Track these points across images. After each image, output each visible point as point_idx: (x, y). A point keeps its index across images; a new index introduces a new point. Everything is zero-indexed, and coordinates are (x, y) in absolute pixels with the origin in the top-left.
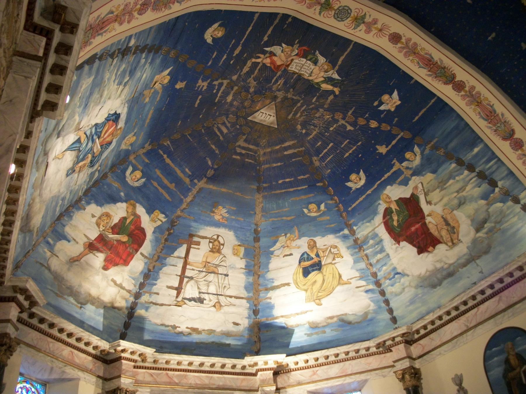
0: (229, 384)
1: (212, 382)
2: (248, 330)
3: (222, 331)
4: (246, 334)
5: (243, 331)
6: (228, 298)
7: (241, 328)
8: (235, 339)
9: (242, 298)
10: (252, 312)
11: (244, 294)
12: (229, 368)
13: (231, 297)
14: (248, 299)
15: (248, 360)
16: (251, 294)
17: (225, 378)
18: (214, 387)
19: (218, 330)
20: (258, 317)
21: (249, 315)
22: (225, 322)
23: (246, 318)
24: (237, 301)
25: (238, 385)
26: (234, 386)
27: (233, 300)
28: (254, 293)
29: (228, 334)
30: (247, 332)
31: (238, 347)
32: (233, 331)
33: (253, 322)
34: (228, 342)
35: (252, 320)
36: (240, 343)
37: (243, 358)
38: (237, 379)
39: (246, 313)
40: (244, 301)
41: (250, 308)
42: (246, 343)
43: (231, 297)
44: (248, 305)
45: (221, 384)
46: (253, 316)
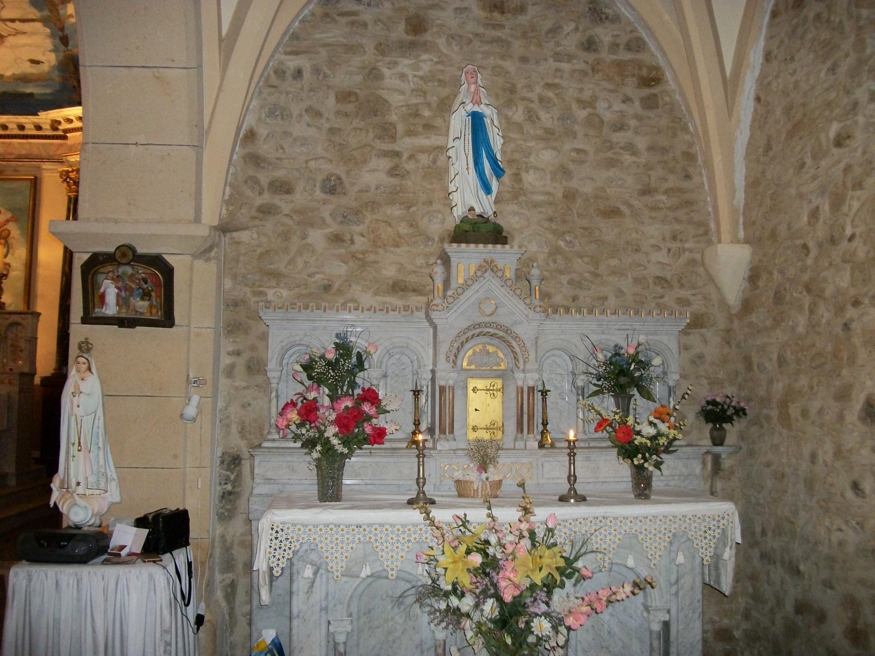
0: (35, 151)
1: (9, 150)
2: (59, 70)
3: (14, 74)
4: (56, 76)
5: (49, 72)
6: (9, 23)
7: (45, 68)
8: (39, 86)
9: (33, 20)
10: (57, 41)
11: (33, 13)
12: (30, 129)
13: (13, 21)
14: (45, 21)
15: (45, 117)
16: (46, 13)
17: (30, 144)
18: (12, 157)
19: (8, 73)
20: (69, 48)
21: (55, 46)
22: (15, 61)
23: (50, 51)
24: (27, 27)
25: (51, 153)
26: (44, 154)
27: (18, 25)
28: (51, 11)
29: (25, 79)
30: (56, 73)
31: (50, 97)
32: (32, 74)
33: (65, 57)
34: (28, 90)
35: (62, 54)
36: (48, 91)
37: (35, 114)
38: (51, 144)
39: (48, 43)
40: (39, 25)
41: (52, 36)
42: (58, 91)
43: (13, 21)
44: (49, 31)
45: (23, 152)
46: (62, 47)
